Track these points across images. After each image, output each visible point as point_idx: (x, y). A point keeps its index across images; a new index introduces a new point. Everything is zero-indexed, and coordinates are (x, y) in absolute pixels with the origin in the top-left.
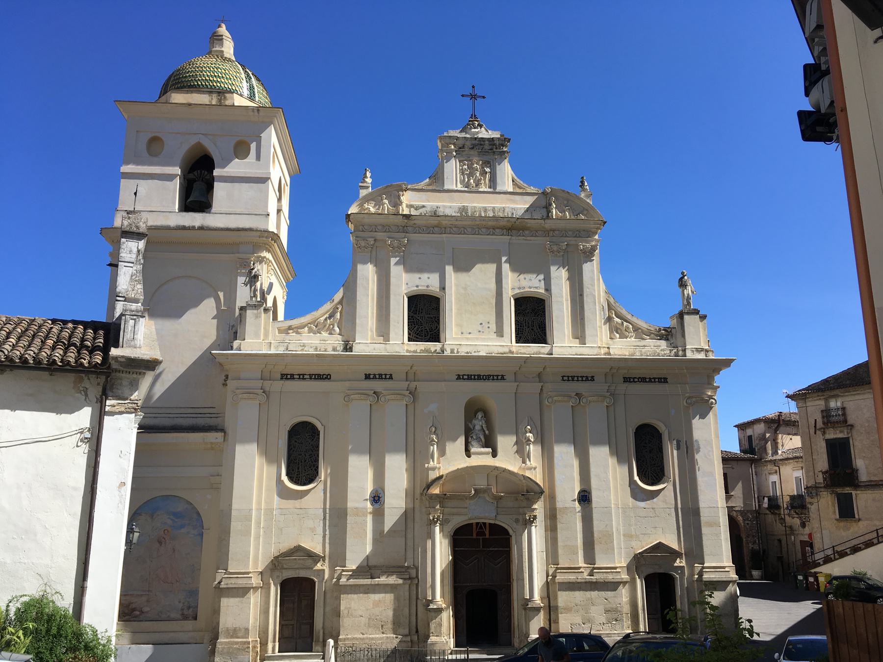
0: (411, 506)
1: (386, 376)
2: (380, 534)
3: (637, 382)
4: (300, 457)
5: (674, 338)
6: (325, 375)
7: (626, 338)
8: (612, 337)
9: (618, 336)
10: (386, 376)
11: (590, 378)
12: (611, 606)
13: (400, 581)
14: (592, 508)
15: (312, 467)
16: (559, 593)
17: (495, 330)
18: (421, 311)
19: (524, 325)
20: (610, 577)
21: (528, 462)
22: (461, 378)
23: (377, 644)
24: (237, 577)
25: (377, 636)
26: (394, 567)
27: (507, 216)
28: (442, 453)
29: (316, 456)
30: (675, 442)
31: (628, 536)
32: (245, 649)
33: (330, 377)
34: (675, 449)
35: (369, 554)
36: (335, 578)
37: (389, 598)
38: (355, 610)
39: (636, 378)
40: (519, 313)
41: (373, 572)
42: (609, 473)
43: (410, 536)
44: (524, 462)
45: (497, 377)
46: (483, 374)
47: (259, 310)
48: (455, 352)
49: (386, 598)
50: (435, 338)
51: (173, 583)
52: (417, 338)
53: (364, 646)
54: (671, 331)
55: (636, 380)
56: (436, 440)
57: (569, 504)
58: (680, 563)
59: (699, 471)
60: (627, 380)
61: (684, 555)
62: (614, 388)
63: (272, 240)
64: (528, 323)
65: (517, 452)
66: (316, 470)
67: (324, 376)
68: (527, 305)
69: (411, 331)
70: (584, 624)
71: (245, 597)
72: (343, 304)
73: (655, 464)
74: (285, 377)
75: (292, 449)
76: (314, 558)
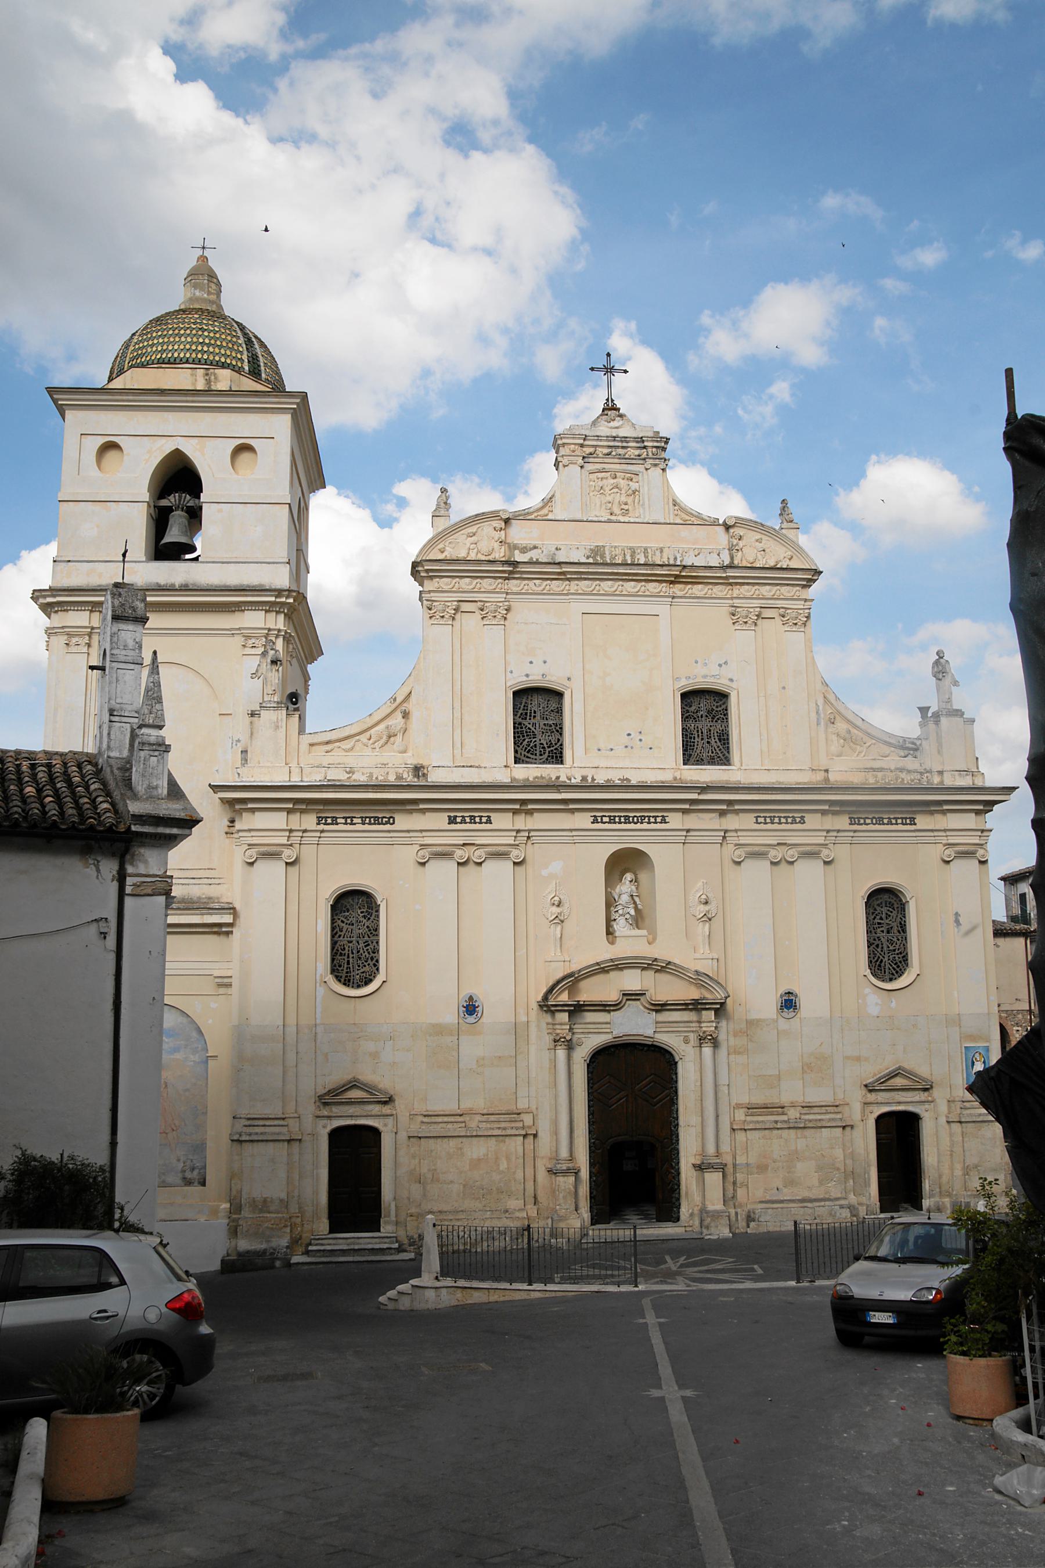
1: (481, 820)
3: (869, 824)
4: (350, 945)
10: (481, 820)
15: (369, 961)
18: (533, 714)
19: (696, 736)
22: (599, 820)
27: (667, 563)
29: (375, 943)
33: (394, 821)
40: (687, 717)
45: (656, 820)
48: (590, 780)
49: (489, 1156)
50: (556, 757)
51: (167, 1133)
52: (528, 757)
54: (921, 745)
55: (868, 821)
64: (702, 733)
66: (375, 965)
67: (384, 820)
69: (519, 746)
73: (894, 950)
74: (323, 821)
75: (337, 933)
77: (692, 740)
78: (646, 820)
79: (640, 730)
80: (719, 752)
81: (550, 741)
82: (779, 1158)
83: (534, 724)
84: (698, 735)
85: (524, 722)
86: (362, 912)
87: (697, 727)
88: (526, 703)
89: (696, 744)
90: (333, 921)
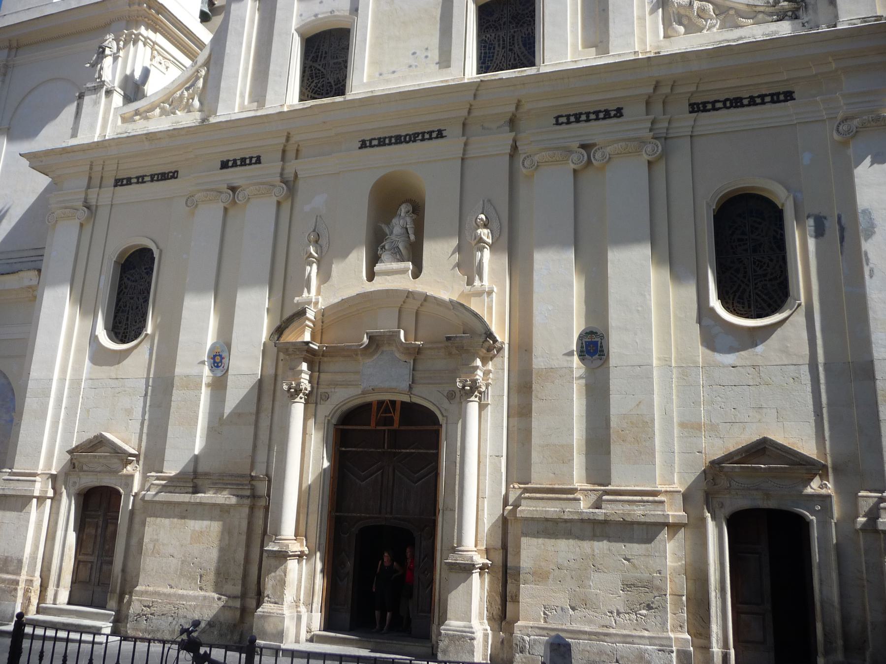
0: (271, 371)
1: (251, 160)
2: (220, 419)
4: (132, 301)
5: (810, 11)
6: (171, 172)
7: (701, 30)
8: (670, 33)
9: (681, 29)
11: (613, 113)
12: (638, 575)
13: (233, 500)
14: (609, 368)
16: (524, 540)
17: (437, 59)
18: (324, 55)
19: (497, 46)
20: (638, 513)
21: (477, 283)
22: (368, 145)
23: (188, 607)
24: (18, 480)
25: (191, 593)
26: (232, 476)
28: (325, 276)
30: (811, 222)
31: (692, 428)
32: (11, 591)
34: (811, 236)
35: (201, 453)
36: (145, 489)
37: (214, 527)
38: (163, 545)
39: (718, 101)
41: (199, 482)
42: (650, 295)
43: (264, 423)
44: (470, 282)
46: (404, 134)
47: (99, 94)
49: (212, 528)
53: (166, 609)
56: (316, 255)
57: (559, 361)
58: (821, 487)
59: (871, 277)
60: (696, 108)
61: (830, 470)
62: (666, 125)
63: (150, 8)
64: (504, 41)
65: (458, 265)
68: (502, 11)
70: (573, 609)
71: (24, 511)
72: (211, 68)
75: (122, 290)
76: (124, 458)
77: (492, 51)
78: (420, 137)
79: (426, 47)
80: (522, 58)
81: (338, 78)
82: (566, 563)
83: (324, 66)
84: (499, 45)
85: (315, 65)
86: (145, 269)
87: (499, 36)
88: (318, 46)
89: (495, 55)
90: (121, 279)
